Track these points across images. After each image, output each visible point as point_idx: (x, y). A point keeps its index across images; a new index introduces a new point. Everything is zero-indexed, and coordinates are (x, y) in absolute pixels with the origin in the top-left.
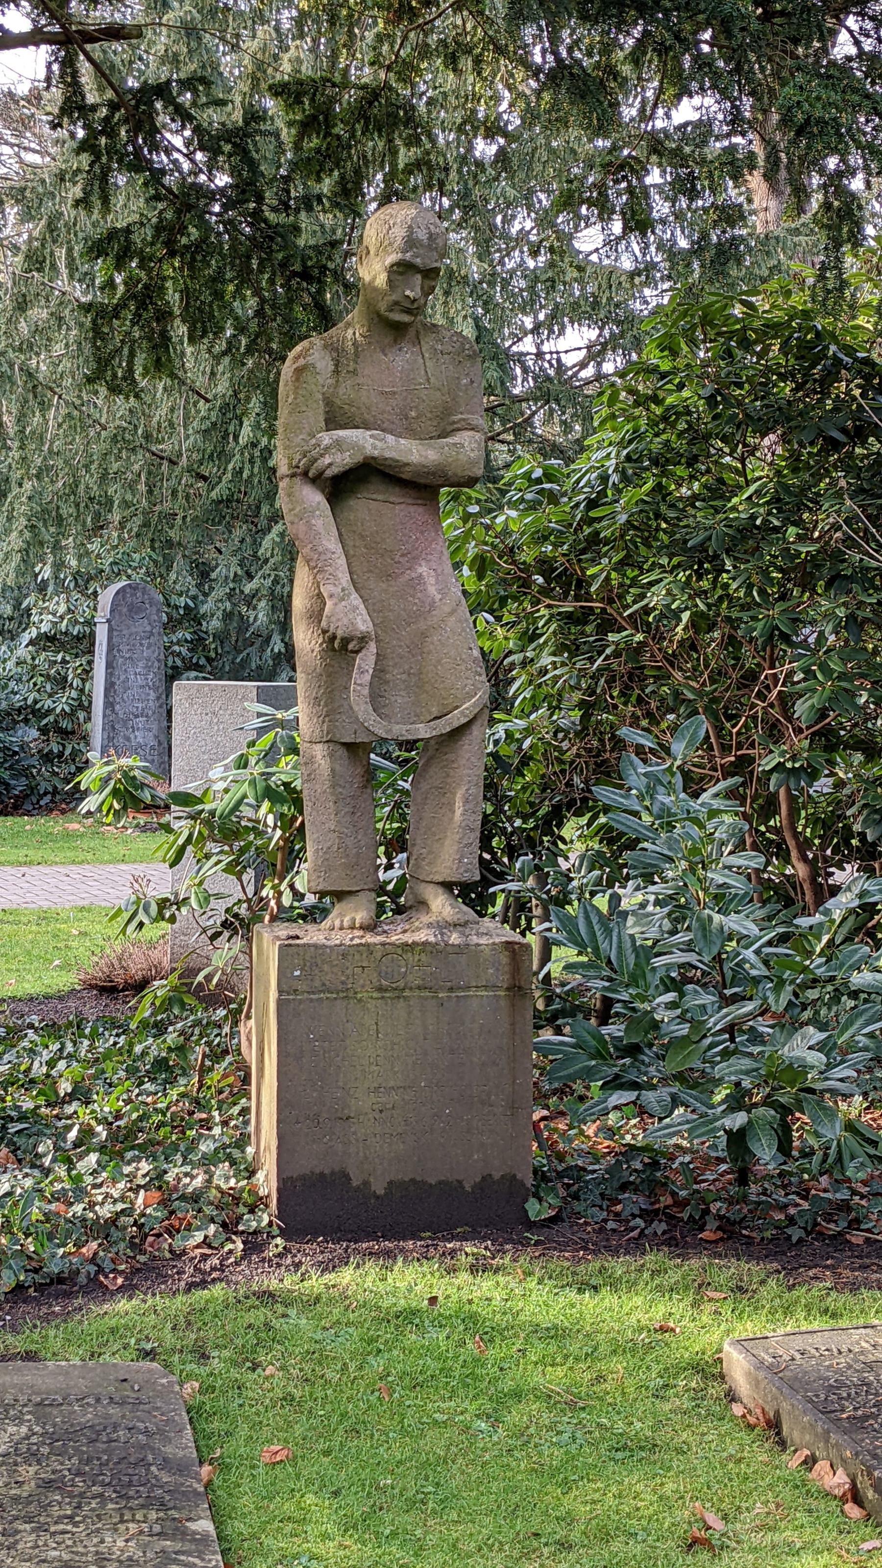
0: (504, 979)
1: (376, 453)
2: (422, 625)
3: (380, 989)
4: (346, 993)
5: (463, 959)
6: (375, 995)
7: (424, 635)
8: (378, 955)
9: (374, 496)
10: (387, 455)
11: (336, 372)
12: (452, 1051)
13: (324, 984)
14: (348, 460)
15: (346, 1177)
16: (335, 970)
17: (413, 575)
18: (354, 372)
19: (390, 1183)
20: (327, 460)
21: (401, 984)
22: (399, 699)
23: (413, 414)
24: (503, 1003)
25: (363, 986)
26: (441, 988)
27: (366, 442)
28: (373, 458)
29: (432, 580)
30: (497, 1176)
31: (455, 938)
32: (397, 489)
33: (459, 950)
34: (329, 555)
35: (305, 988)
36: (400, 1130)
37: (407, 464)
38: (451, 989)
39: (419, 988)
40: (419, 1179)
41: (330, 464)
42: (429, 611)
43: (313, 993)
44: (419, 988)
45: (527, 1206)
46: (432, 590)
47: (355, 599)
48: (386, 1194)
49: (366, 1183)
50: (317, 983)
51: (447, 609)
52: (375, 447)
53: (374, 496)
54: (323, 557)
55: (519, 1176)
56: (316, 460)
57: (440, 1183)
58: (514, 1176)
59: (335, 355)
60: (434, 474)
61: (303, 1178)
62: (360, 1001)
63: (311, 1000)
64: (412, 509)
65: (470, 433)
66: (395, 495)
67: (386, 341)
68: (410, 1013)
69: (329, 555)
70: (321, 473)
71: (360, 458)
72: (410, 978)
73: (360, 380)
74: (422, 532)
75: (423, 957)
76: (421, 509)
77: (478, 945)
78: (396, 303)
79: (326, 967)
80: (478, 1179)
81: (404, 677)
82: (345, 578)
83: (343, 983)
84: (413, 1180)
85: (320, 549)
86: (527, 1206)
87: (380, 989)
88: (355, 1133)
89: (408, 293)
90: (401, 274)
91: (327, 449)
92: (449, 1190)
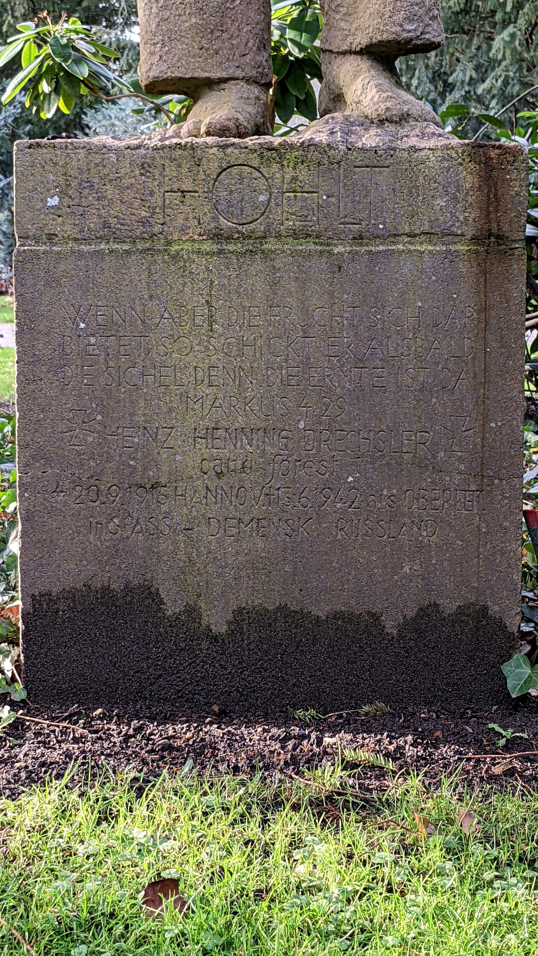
0: (466, 219)
3: (217, 236)
4: (149, 241)
5: (383, 177)
6: (207, 247)
8: (214, 167)
12: (360, 362)
13: (106, 225)
15: (155, 597)
16: (128, 195)
19: (240, 611)
21: (259, 227)
24: (463, 267)
25: (183, 230)
26: (339, 237)
30: (449, 606)
31: (370, 139)
33: (375, 160)
35: (69, 230)
36: (255, 513)
38: (359, 238)
39: (295, 235)
40: (294, 607)
43: (86, 241)
44: (295, 235)
45: (507, 668)
48: (232, 633)
49: (192, 611)
50: (93, 222)
55: (495, 609)
57: (337, 616)
58: (485, 609)
61: (71, 595)
62: (176, 257)
63: (81, 255)
68: (275, 284)
72: (277, 214)
75: (303, 173)
77: (416, 149)
79: (110, 191)
80: (410, 613)
83: (144, 222)
84: (282, 609)
86: (507, 668)
87: (217, 236)
88: (167, 515)
92: (355, 633)
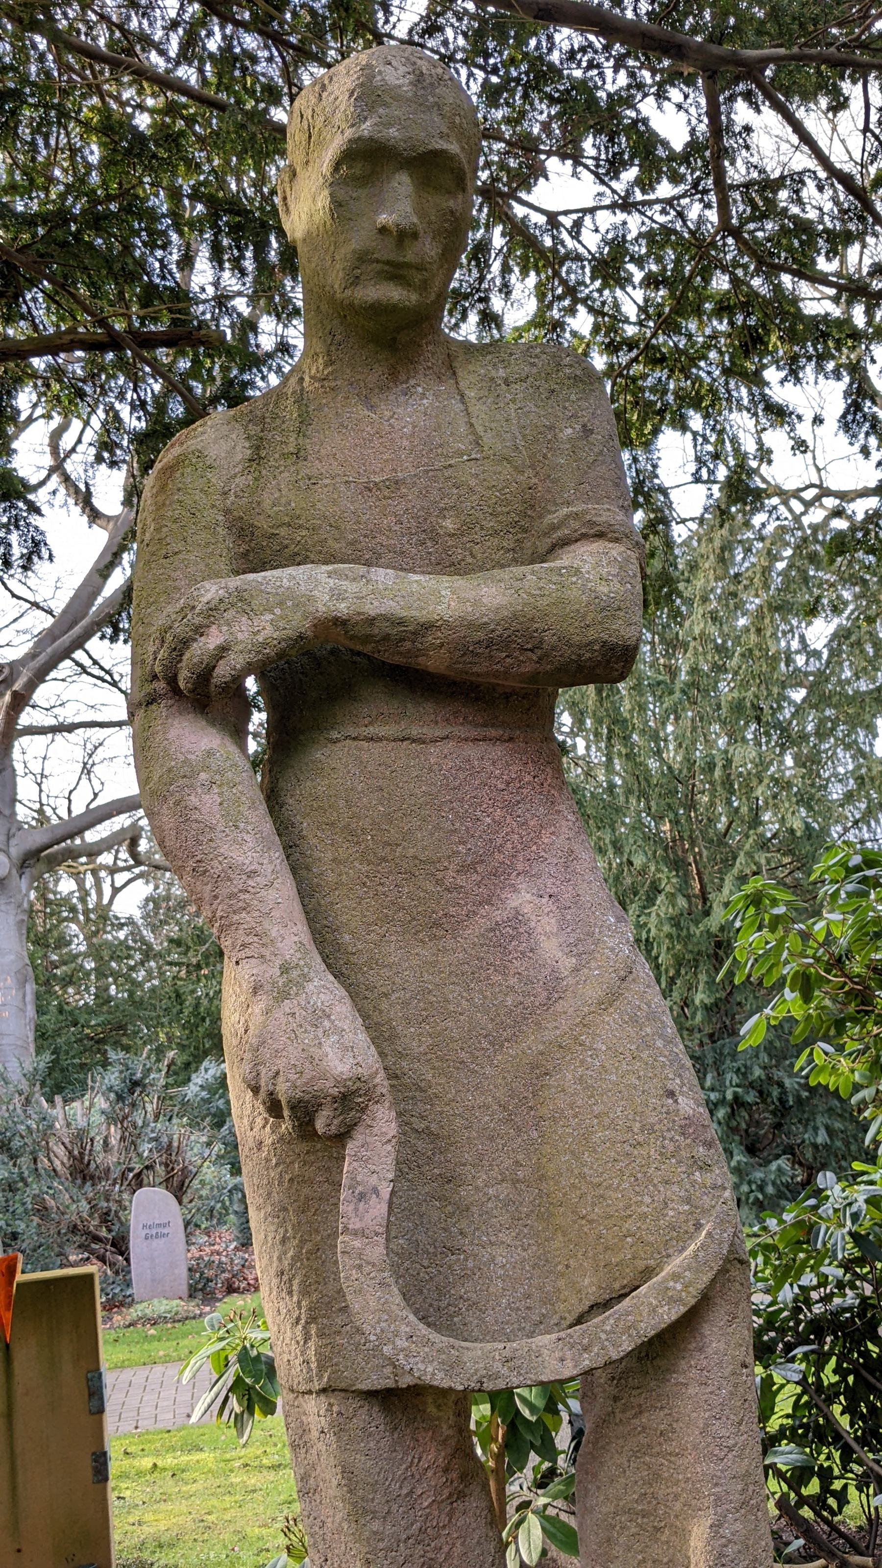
1: (343, 608)
2: (531, 1044)
7: (539, 1071)
9: (372, 730)
10: (372, 608)
11: (256, 459)
14: (269, 631)
17: (498, 915)
18: (298, 455)
20: (213, 640)
22: (499, 1256)
23: (449, 524)
27: (322, 590)
28: (339, 622)
29: (549, 924)
32: (429, 707)
34: (239, 882)
37: (428, 627)
41: (223, 649)
42: (546, 1005)
46: (552, 948)
47: (323, 990)
51: (593, 992)
52: (338, 595)
53: (372, 730)
54: (223, 891)
56: (185, 643)
59: (254, 429)
60: (505, 643)
64: (472, 751)
65: (598, 546)
66: (422, 720)
67: (372, 378)
69: (239, 882)
70: (204, 675)
71: (298, 623)
73: (313, 467)
74: (509, 807)
76: (498, 751)
78: (362, 258)
81: (504, 1190)
82: (291, 936)
85: (216, 868)
89: (383, 218)
90: (363, 181)
91: (213, 612)
